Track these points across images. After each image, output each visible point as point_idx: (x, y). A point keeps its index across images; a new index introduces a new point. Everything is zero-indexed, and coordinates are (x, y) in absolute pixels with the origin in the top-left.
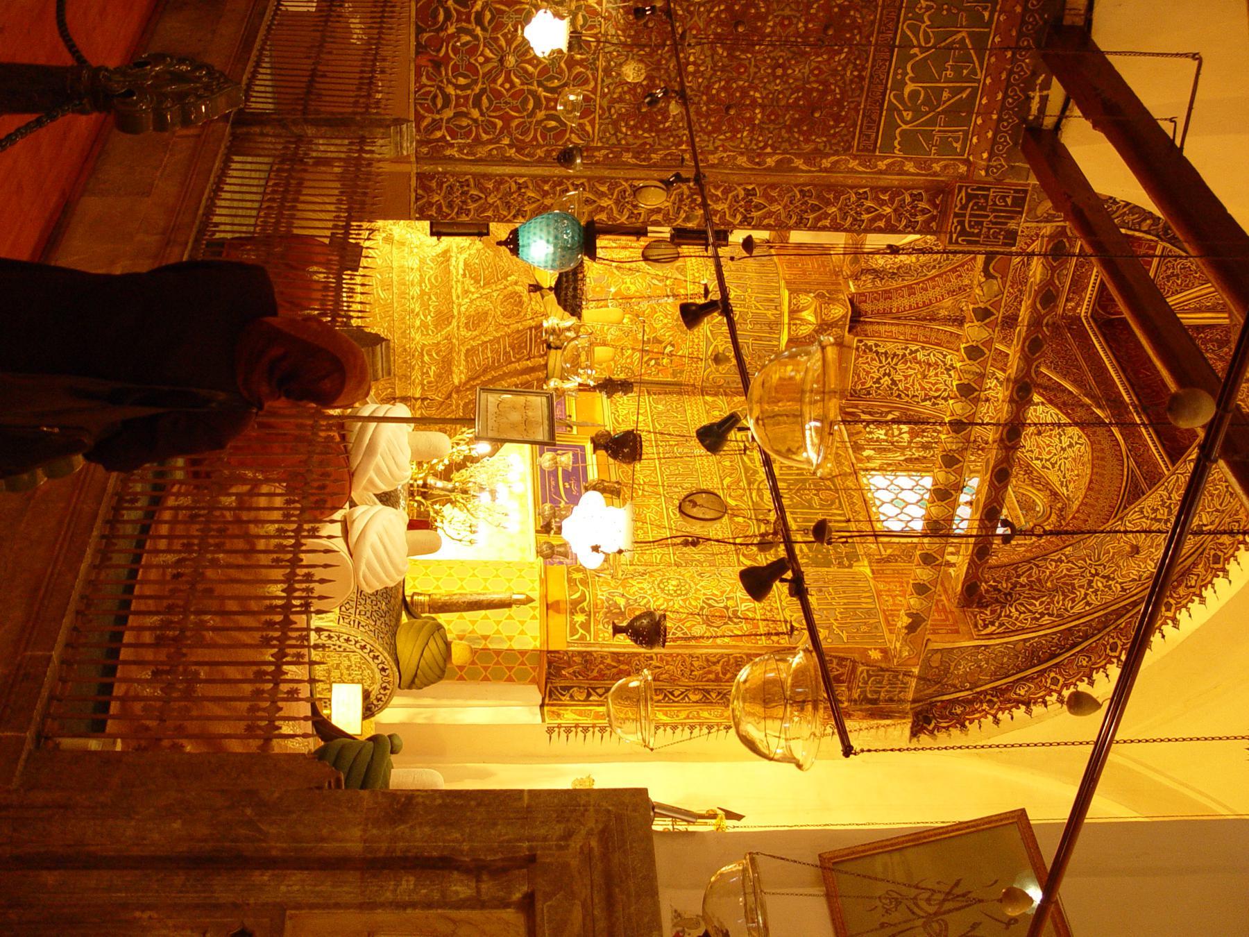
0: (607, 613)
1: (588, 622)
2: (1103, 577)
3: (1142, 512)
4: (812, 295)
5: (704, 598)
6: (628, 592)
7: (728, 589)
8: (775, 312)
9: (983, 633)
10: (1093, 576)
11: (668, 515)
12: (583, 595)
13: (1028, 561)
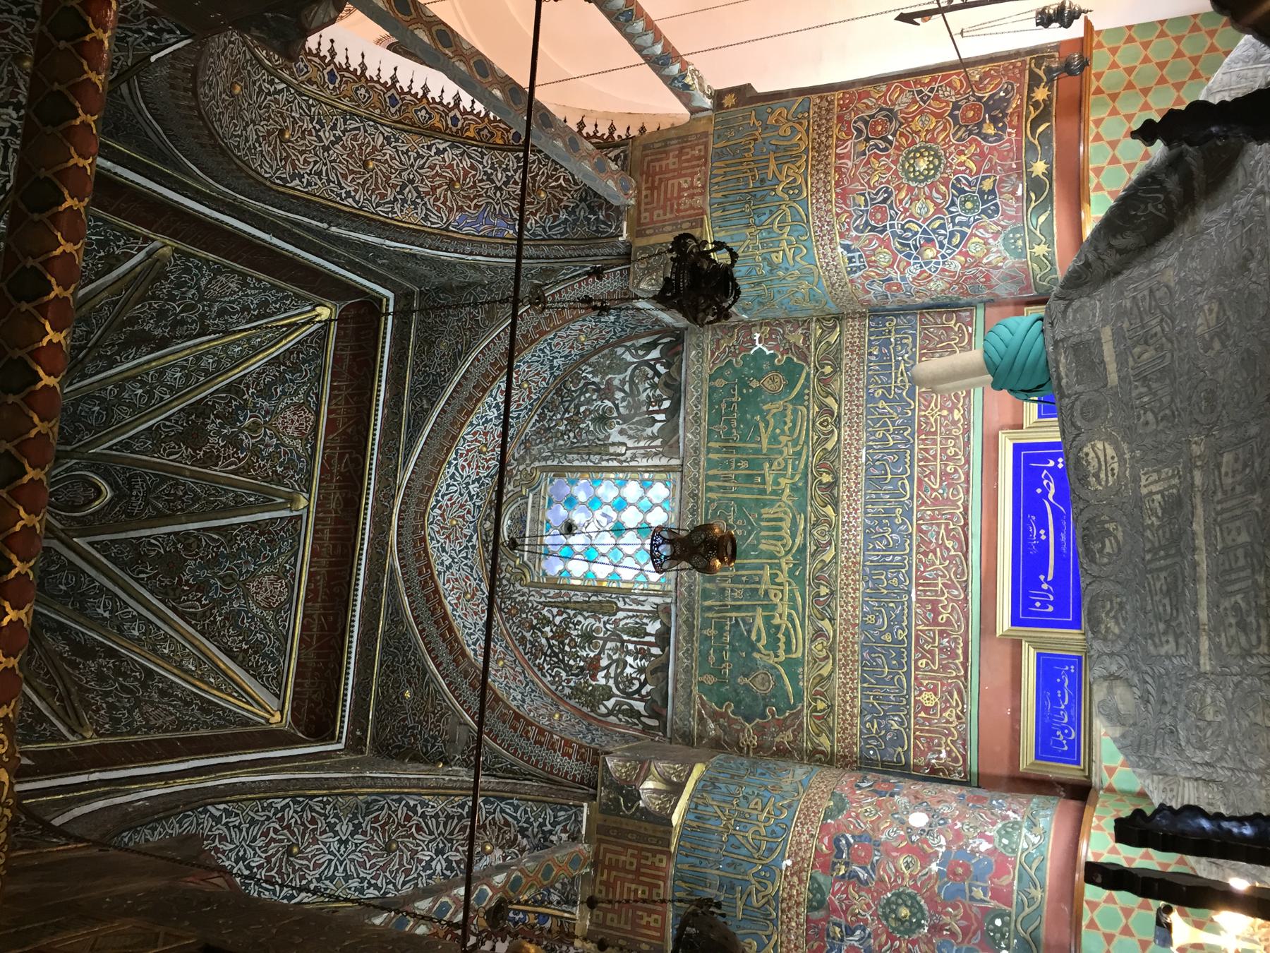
0: (1006, 107)
1: (1031, 90)
2: (493, 182)
3: (426, 215)
4: (642, 804)
5: (892, 151)
6: (979, 144)
7: (861, 170)
8: (700, 801)
9: (622, 148)
10: (500, 189)
11: (912, 489)
12: (1033, 132)
13: (550, 238)
